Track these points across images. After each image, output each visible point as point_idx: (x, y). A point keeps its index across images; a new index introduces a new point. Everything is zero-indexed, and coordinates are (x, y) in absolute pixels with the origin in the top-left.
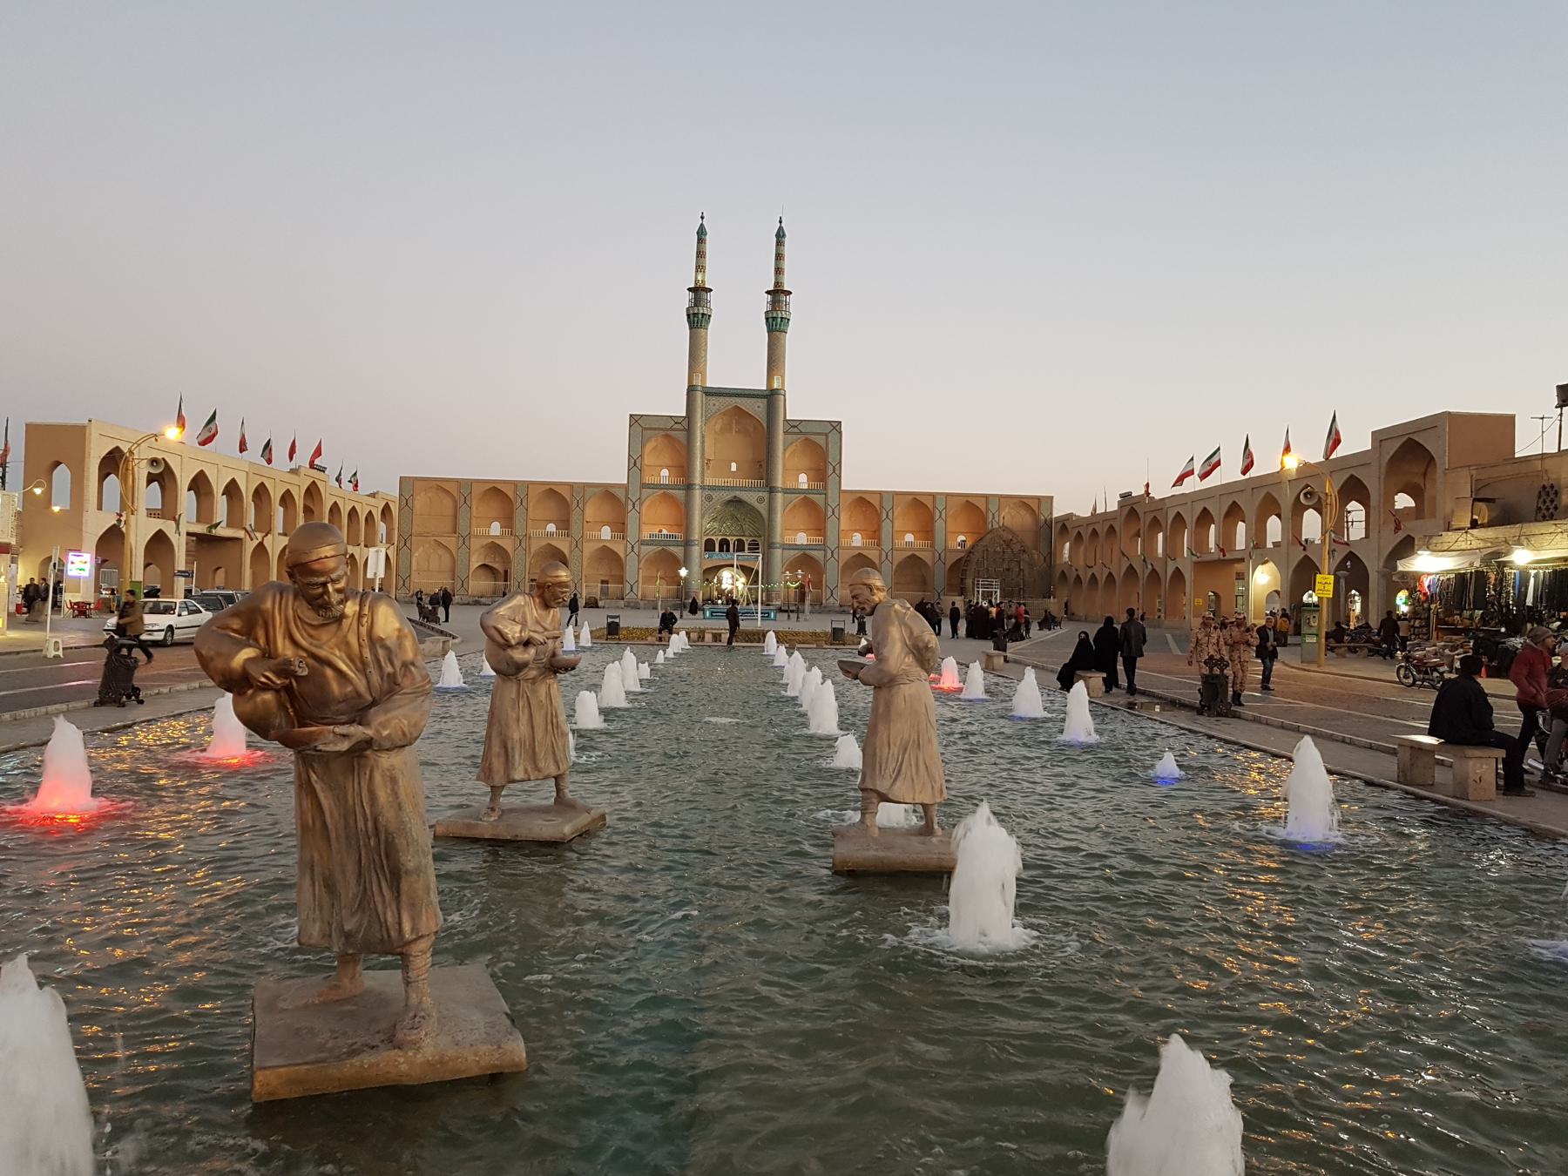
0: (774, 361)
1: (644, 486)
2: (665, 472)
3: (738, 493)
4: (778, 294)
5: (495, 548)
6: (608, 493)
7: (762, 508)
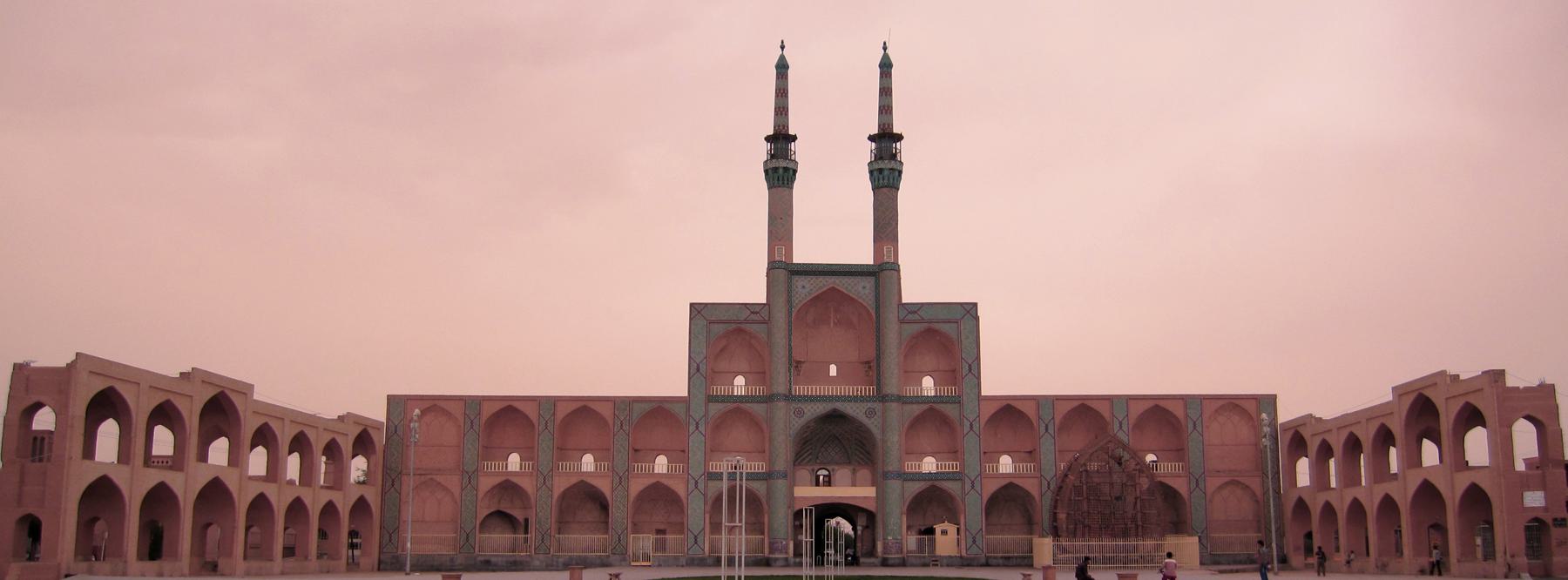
0: (885, 226)
1: (712, 399)
2: (740, 381)
3: (840, 406)
4: (886, 140)
5: (508, 487)
6: (657, 411)
7: (873, 425)
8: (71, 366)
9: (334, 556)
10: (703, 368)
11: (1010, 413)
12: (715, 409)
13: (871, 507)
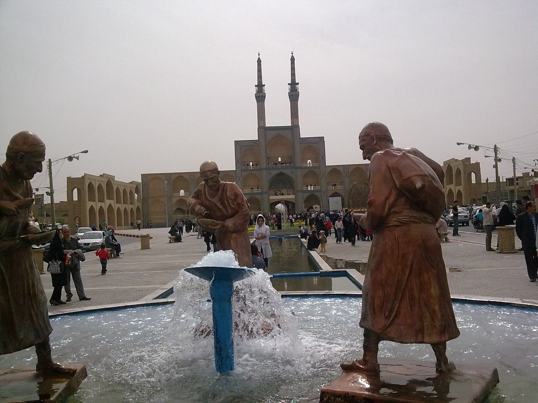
8: (83, 177)
9: (121, 225)
10: (240, 161)
11: (335, 170)
12: (244, 173)
13: (293, 201)
